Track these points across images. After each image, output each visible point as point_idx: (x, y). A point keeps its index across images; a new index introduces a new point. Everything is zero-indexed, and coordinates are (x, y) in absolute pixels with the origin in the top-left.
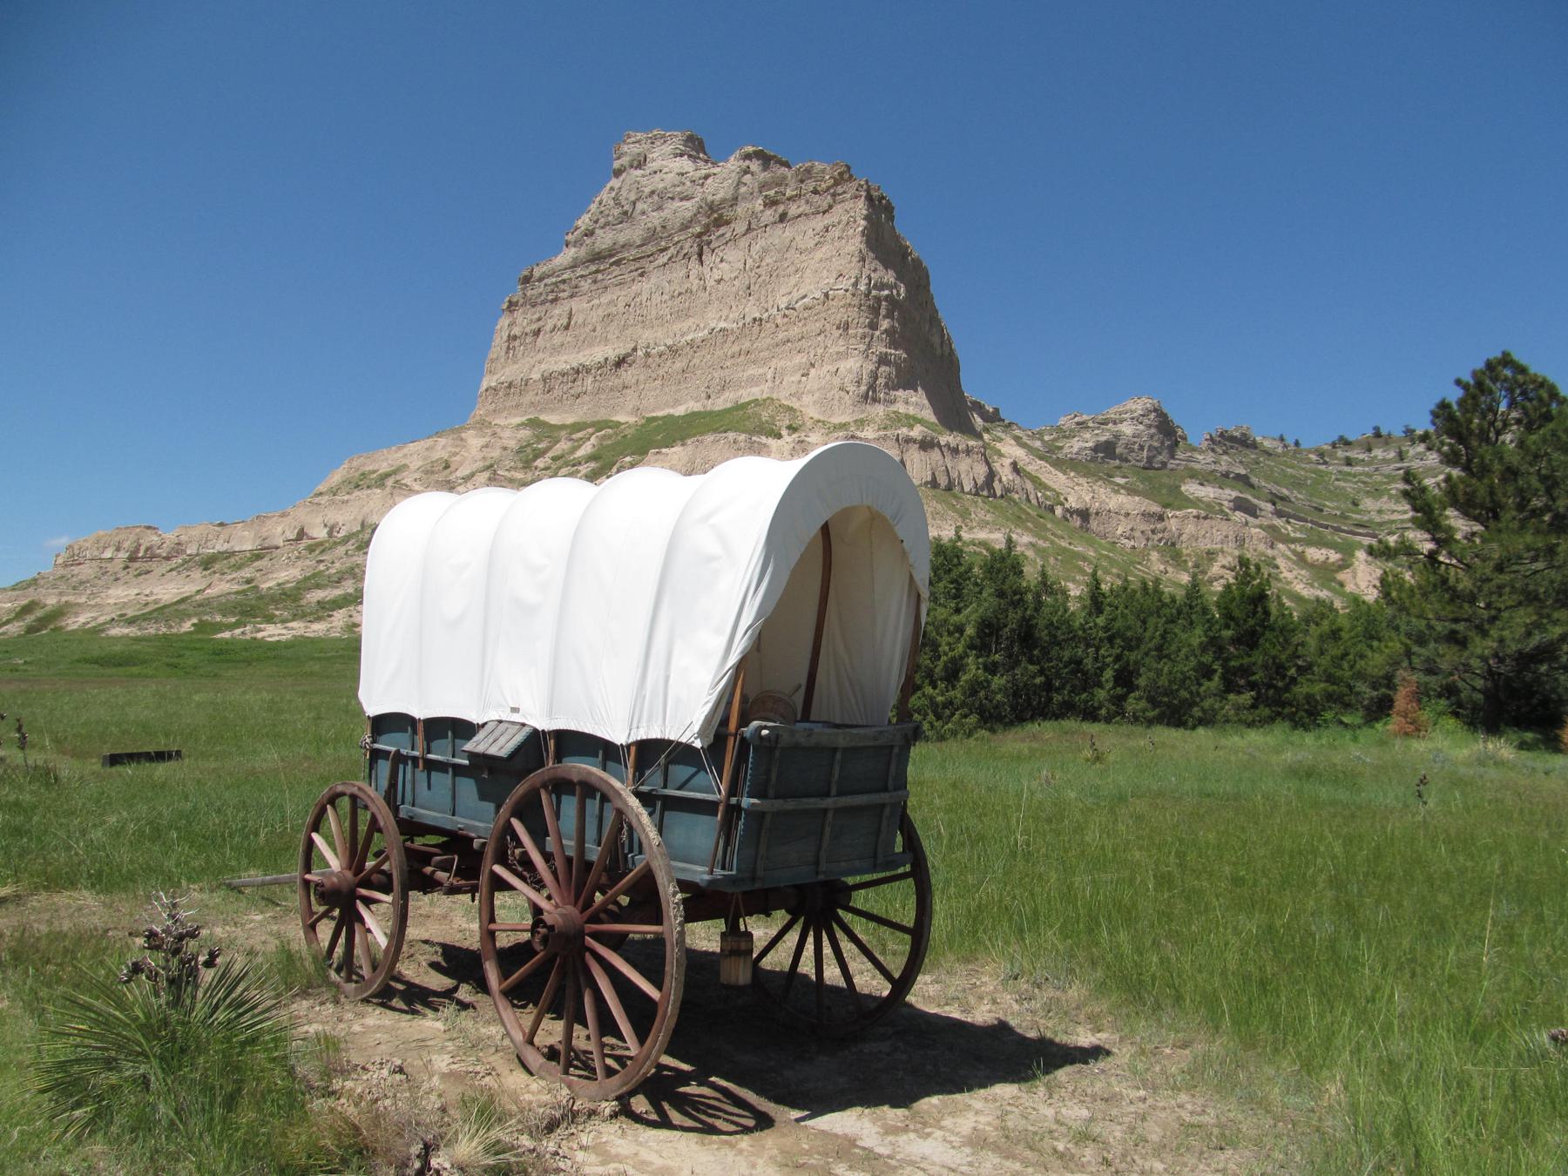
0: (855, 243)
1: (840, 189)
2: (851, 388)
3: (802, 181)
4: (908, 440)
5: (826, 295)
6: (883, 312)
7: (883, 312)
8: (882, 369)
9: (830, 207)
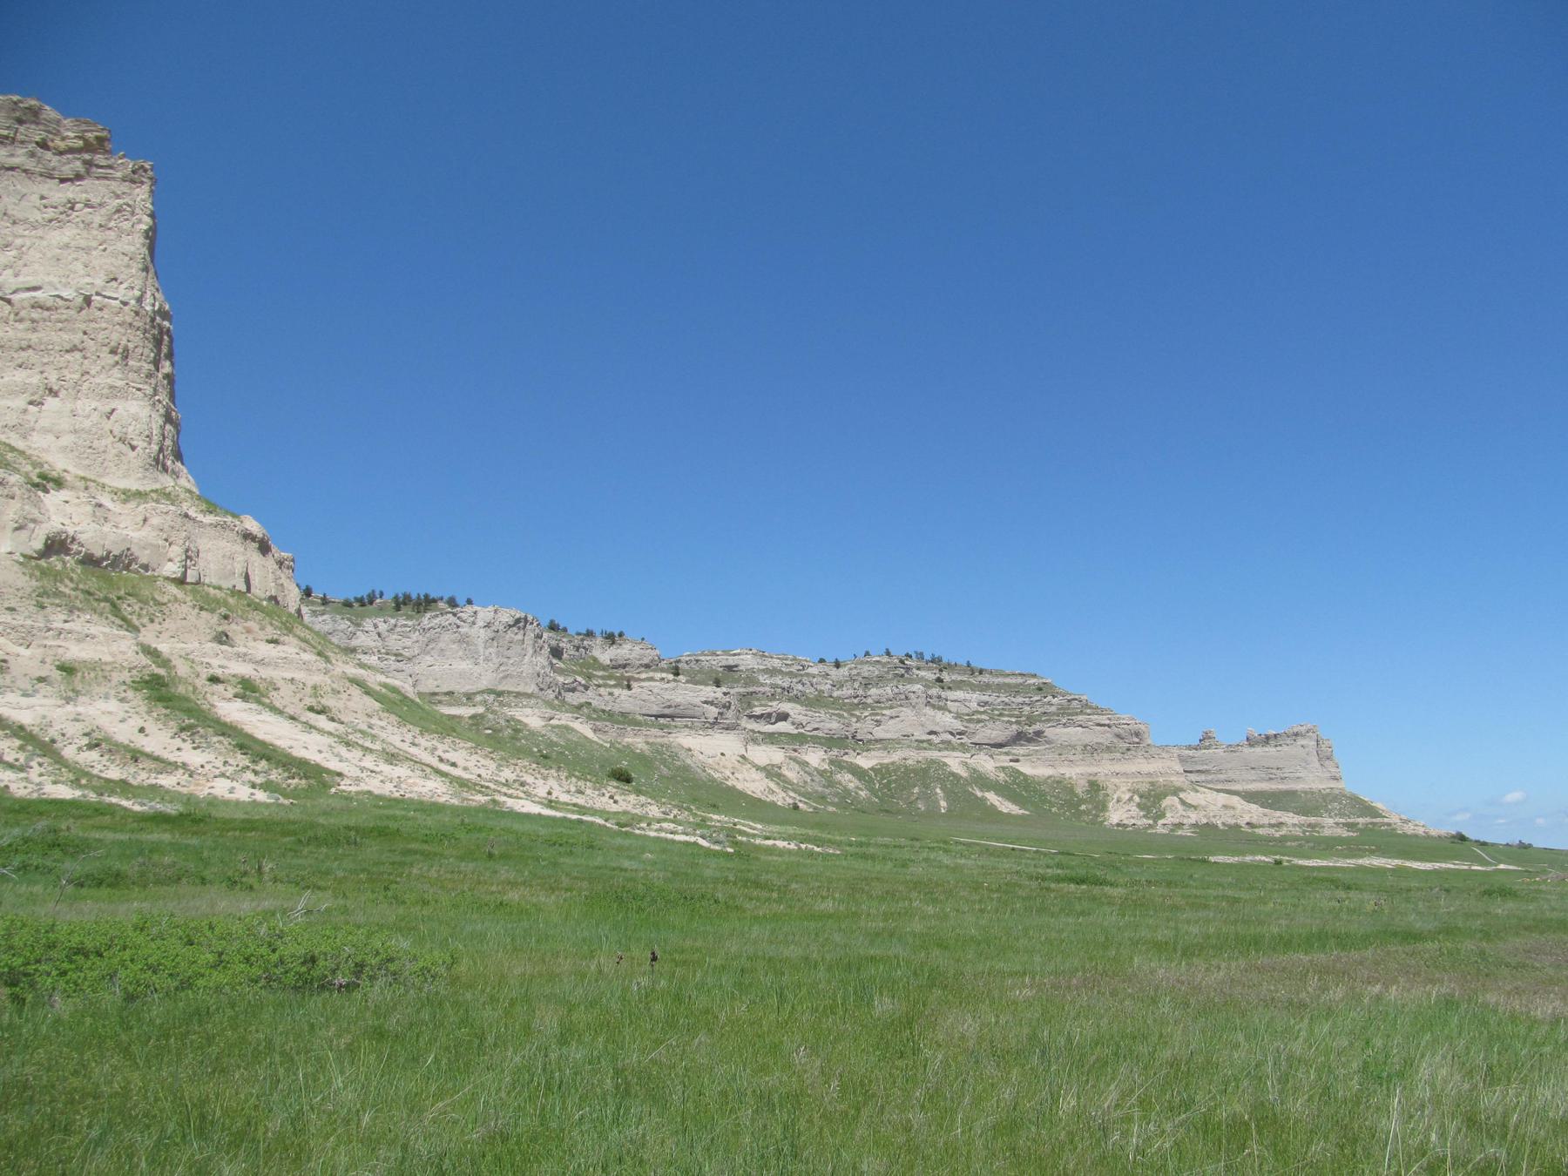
0: (135, 244)
1: (100, 159)
2: (140, 443)
3: (20, 122)
4: (248, 536)
5: (88, 301)
6: (165, 350)
7: (165, 350)
8: (168, 427)
9: (79, 177)
